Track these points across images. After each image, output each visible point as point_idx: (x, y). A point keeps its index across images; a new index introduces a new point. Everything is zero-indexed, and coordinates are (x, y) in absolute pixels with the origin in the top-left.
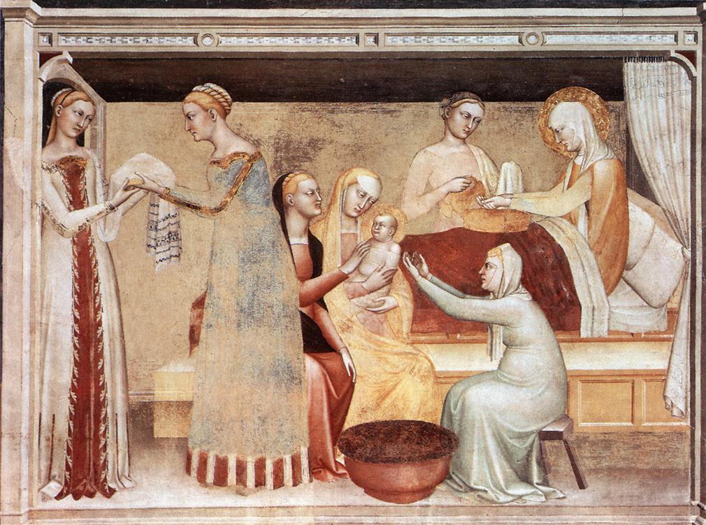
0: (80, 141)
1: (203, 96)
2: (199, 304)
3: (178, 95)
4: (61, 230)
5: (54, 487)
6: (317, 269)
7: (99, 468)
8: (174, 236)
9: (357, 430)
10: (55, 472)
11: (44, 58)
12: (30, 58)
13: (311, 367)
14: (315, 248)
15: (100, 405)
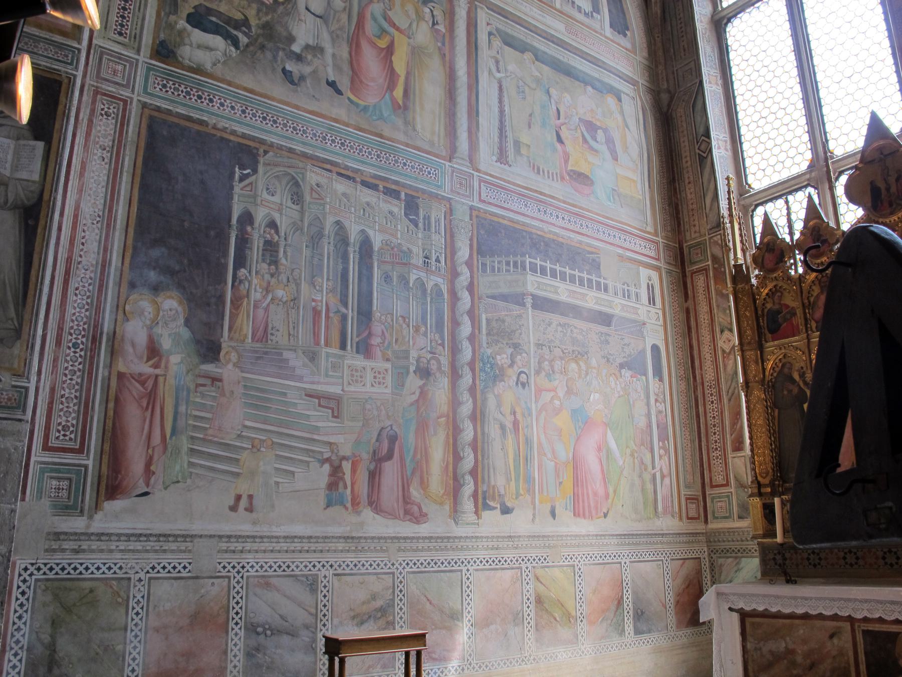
0: (498, 52)
1: (528, 56)
2: (530, 115)
3: (522, 52)
4: (495, 77)
5: (495, 158)
6: (559, 119)
7: (507, 157)
8: (523, 92)
9: (572, 171)
10: (495, 153)
11: (488, 24)
12: (484, 24)
13: (558, 146)
14: (558, 111)
15: (506, 137)
